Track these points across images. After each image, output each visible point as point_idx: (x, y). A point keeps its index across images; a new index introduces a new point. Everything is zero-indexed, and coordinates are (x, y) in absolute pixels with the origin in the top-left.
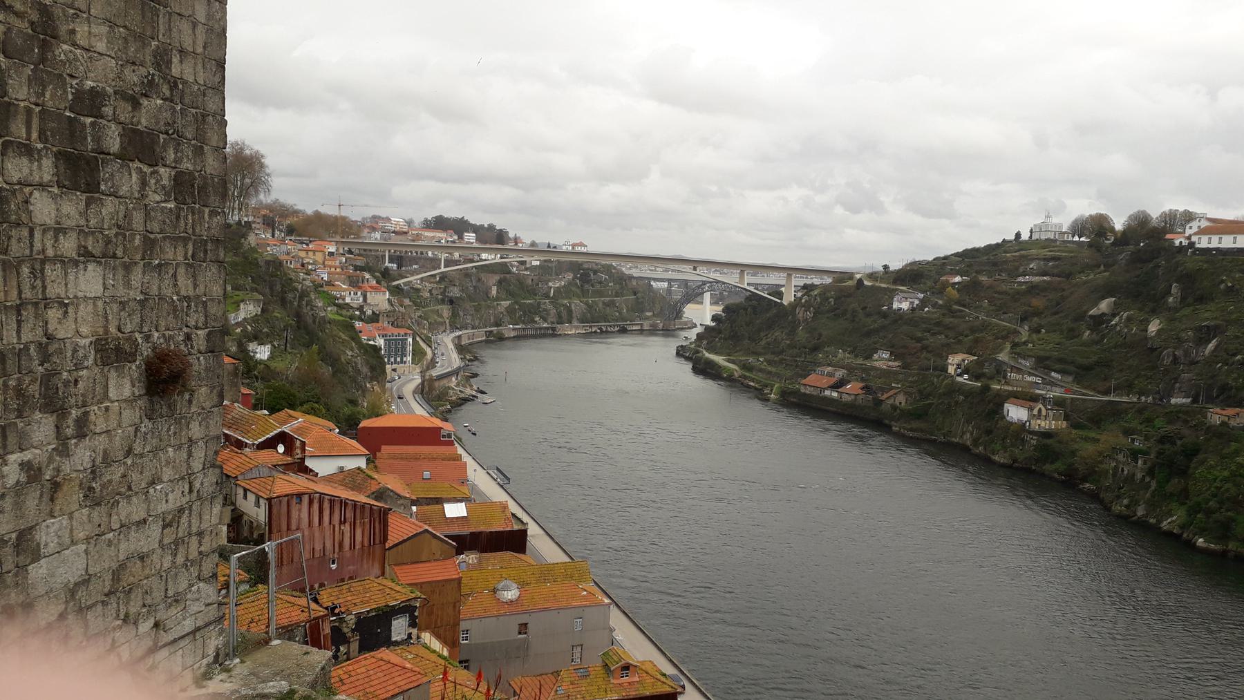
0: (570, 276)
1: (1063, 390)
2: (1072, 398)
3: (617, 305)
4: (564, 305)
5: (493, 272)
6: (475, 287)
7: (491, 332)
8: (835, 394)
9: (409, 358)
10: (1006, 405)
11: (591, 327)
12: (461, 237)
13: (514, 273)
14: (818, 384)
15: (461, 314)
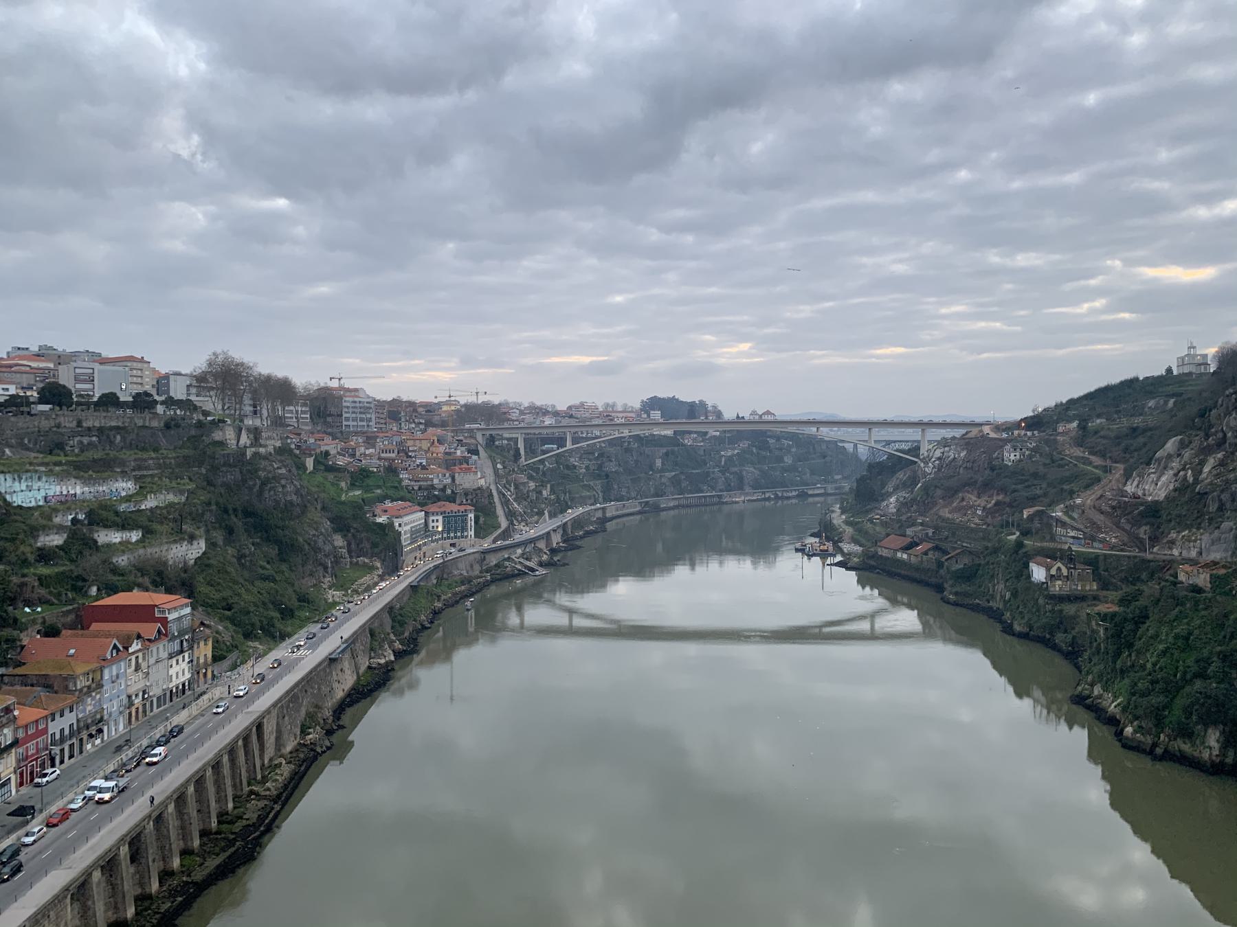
0: (744, 444)
1: (1101, 546)
2: (1105, 555)
3: (800, 469)
4: (735, 473)
5: (661, 446)
6: (636, 461)
7: (647, 502)
8: (905, 556)
9: (472, 533)
10: (1031, 564)
11: (763, 493)
12: (649, 416)
13: (683, 445)
14: (892, 546)
15: (616, 487)
